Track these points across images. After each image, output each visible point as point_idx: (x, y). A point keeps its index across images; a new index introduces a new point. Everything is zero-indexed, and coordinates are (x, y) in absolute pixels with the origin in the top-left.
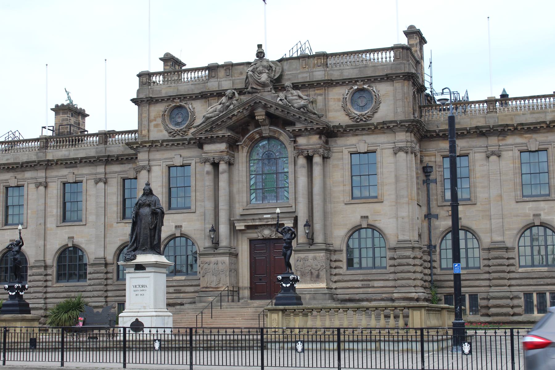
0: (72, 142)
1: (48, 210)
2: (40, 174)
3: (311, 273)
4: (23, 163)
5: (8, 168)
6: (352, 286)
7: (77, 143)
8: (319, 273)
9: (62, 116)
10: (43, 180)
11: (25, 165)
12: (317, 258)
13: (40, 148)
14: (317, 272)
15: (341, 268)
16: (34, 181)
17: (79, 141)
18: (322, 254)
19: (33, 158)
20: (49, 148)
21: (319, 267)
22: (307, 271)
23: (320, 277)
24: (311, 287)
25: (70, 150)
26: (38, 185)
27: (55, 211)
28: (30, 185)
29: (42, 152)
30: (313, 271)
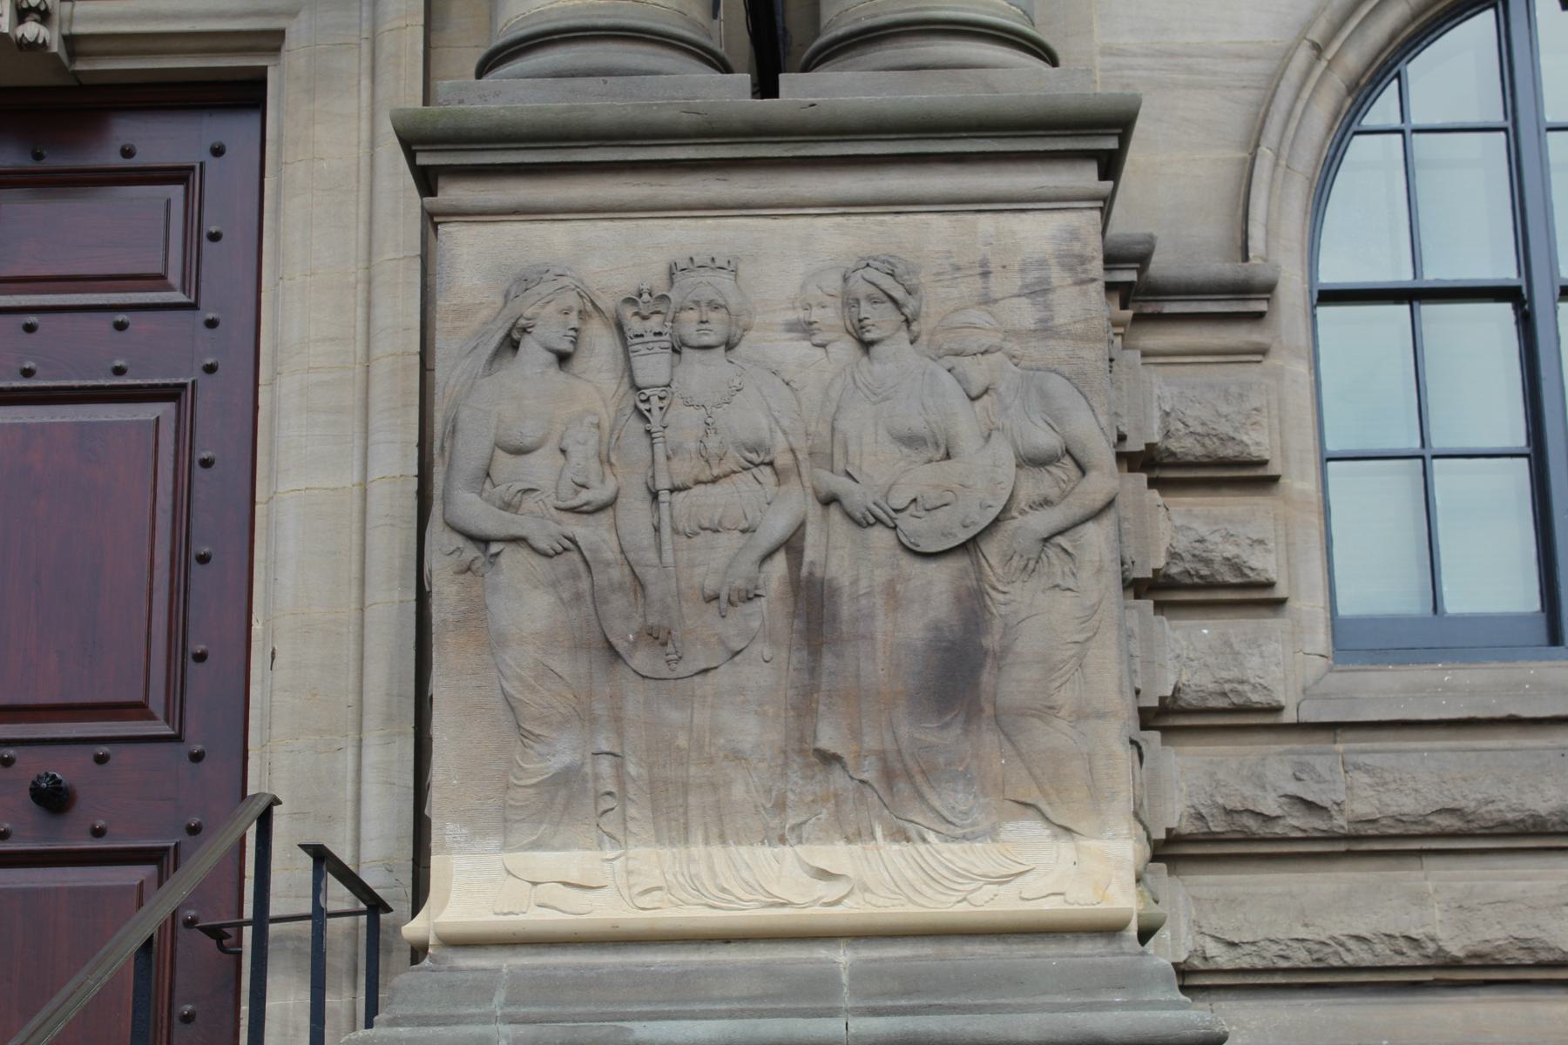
3: (814, 610)
6: (1489, 932)
8: (973, 607)
12: (939, 300)
14: (940, 579)
15: (1257, 597)
18: (1037, 233)
21: (984, 474)
22: (715, 561)
23: (1013, 684)
24: (810, 903)
30: (837, 554)
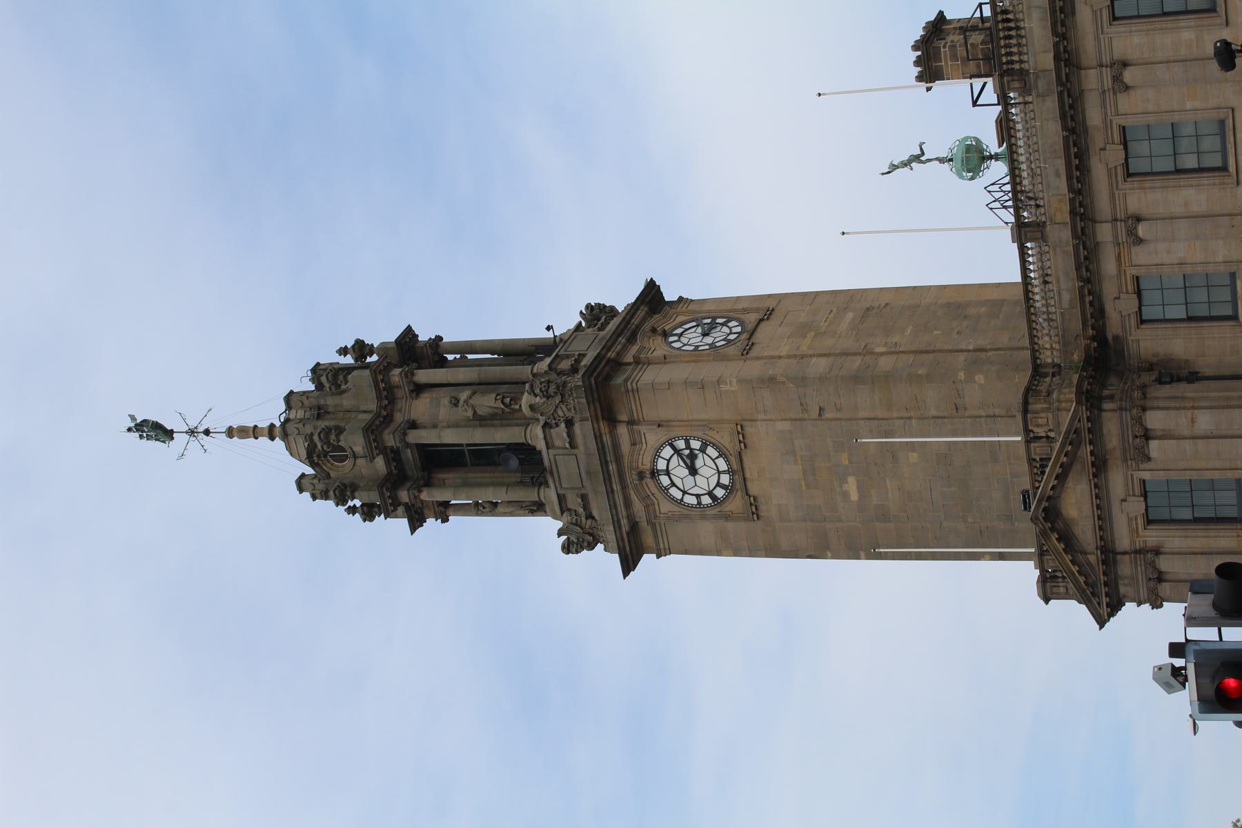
0: (1010, 29)
1: (1183, 52)
2: (1092, 80)
4: (1065, 128)
5: (1077, 168)
7: (1012, 25)
9: (945, 63)
10: (1107, 74)
11: (1070, 124)
13: (1025, 90)
16: (1109, 97)
17: (1008, 20)
19: (1052, 103)
20: (1025, 66)
25: (1029, 8)
26: (1120, 85)
27: (1187, 35)
28: (1122, 109)
29: (1036, 82)
